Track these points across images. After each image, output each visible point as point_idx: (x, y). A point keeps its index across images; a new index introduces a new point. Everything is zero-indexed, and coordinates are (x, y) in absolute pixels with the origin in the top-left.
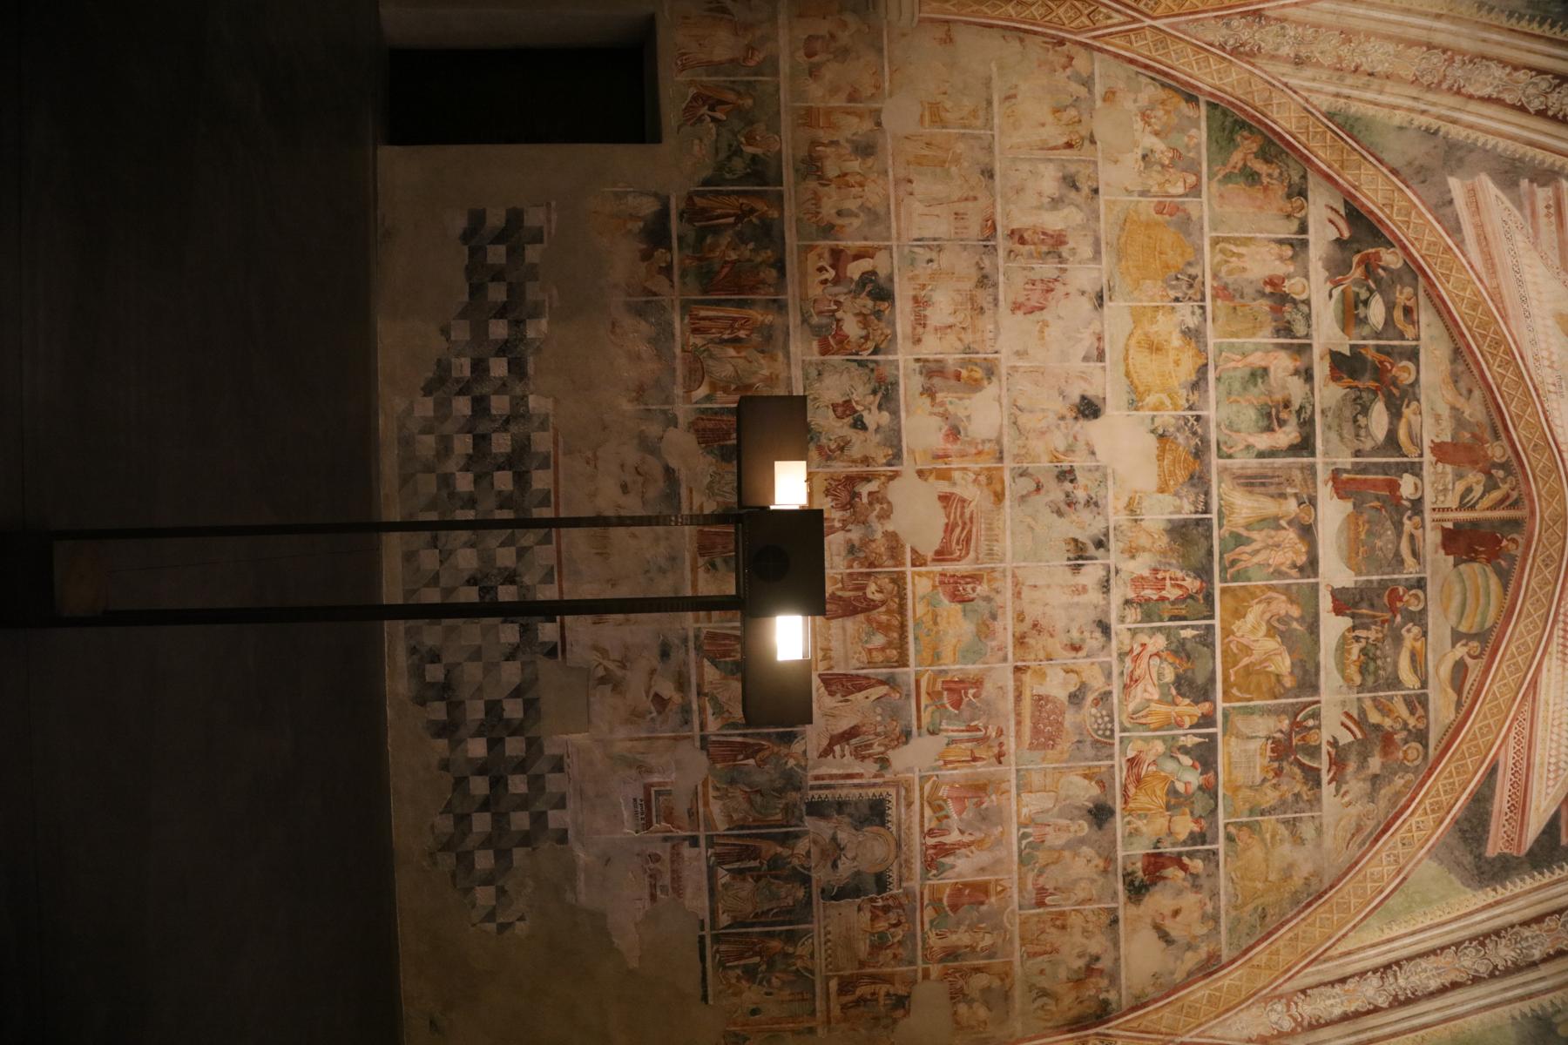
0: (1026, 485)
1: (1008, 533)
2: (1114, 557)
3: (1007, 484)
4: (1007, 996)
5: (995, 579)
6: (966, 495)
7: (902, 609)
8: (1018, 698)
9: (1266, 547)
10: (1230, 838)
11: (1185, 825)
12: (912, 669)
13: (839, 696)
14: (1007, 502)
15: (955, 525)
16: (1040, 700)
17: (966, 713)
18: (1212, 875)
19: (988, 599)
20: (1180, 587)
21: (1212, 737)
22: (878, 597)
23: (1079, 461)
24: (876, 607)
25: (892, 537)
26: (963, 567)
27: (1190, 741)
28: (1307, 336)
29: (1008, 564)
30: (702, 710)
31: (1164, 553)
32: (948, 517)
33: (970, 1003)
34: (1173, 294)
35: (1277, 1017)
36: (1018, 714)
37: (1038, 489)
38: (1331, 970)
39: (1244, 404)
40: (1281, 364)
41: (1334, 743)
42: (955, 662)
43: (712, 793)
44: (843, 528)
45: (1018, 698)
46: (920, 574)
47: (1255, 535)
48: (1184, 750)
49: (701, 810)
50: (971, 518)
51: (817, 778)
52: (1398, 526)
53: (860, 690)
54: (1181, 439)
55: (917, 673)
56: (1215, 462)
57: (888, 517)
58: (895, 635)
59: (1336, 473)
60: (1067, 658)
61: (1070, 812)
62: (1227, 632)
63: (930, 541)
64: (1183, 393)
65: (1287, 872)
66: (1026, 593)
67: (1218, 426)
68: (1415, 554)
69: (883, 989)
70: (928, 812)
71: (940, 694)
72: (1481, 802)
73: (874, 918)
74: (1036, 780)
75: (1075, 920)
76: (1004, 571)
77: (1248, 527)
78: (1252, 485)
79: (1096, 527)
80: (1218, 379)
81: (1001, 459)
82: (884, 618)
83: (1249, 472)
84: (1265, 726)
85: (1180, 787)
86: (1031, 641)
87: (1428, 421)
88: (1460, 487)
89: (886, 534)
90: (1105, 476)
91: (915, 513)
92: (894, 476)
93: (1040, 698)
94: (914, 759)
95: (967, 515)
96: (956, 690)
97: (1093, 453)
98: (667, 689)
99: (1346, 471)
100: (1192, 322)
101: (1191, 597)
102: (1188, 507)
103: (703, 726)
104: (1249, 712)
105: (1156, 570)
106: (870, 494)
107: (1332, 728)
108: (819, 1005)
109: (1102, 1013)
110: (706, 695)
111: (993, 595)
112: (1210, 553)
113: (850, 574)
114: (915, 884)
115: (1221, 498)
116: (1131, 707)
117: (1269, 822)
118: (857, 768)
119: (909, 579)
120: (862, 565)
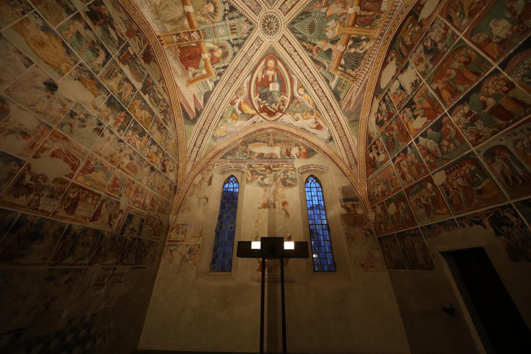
0: (67, 128)
1: (80, 144)
2: (106, 124)
3: (62, 133)
4: (168, 203)
5: (92, 157)
6: (58, 148)
7: (84, 189)
8: (124, 171)
9: (125, 91)
10: (166, 149)
11: (161, 155)
12: (103, 194)
13: (99, 218)
14: (69, 138)
15: (66, 158)
16: (127, 166)
17: (121, 185)
18: (169, 157)
19: (97, 163)
20: (122, 117)
21: (152, 138)
22: (76, 195)
23: (70, 107)
24: (79, 197)
25: (56, 180)
26: (82, 164)
27: (150, 143)
28: (76, 9)
29: (90, 151)
30: (80, 265)
31: (113, 113)
32: (62, 158)
33: (166, 210)
34: (20, 10)
35: (191, 163)
36: (127, 173)
37: (71, 125)
38: (189, 152)
39: (85, 50)
40: (79, 26)
41: (163, 120)
42: (108, 182)
43: (105, 263)
44: (40, 196)
45: (124, 171)
46: (76, 178)
47: (122, 90)
48: (151, 145)
49: (108, 266)
50: (67, 152)
51: (115, 230)
52: (137, 63)
53: (100, 211)
54: (84, 76)
55: (105, 193)
56: (97, 76)
57: (47, 178)
58: (91, 194)
59: (119, 57)
60: (122, 154)
61: (149, 174)
62: (137, 117)
63: (67, 168)
64: (68, 58)
65: (173, 145)
66: (101, 152)
67: (87, 64)
68: (144, 69)
69: (158, 226)
70: (136, 205)
71: (113, 190)
72: (184, 111)
73: (147, 224)
74: (141, 177)
75: (164, 184)
76: (91, 154)
77: (119, 89)
78: (109, 77)
79: (95, 122)
80: (71, 45)
81: (51, 128)
82: (84, 196)
83: (106, 73)
84: (155, 128)
85: (155, 151)
86: (114, 159)
87: (120, 26)
88: (137, 44)
89: (53, 182)
90: (81, 105)
91: (52, 168)
92: (29, 167)
93: (127, 166)
94: (124, 203)
95: (66, 152)
96: (115, 185)
97: (70, 101)
98: (66, 277)
99: (120, 56)
100: (40, 23)
101: (126, 117)
102: (105, 96)
103: (85, 264)
104: (151, 128)
105: (115, 118)
106: (31, 180)
107: (161, 117)
108: (155, 241)
109: (176, 187)
110: (75, 263)
111: (96, 161)
112: (119, 103)
113: (61, 200)
114: (146, 213)
115: (108, 87)
116: (139, 149)
117: (167, 141)
118: (119, 218)
119: (76, 182)
120: (61, 195)
